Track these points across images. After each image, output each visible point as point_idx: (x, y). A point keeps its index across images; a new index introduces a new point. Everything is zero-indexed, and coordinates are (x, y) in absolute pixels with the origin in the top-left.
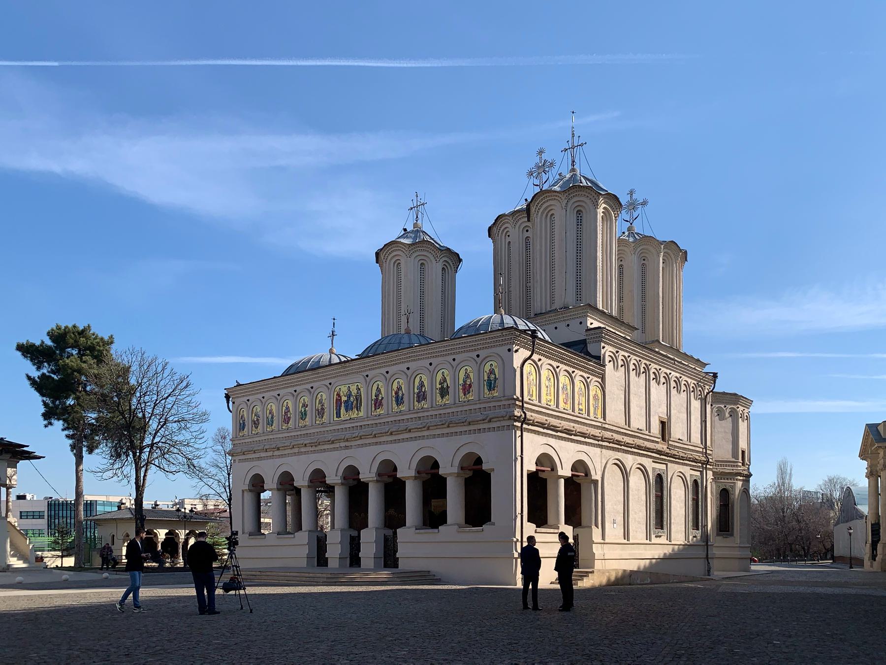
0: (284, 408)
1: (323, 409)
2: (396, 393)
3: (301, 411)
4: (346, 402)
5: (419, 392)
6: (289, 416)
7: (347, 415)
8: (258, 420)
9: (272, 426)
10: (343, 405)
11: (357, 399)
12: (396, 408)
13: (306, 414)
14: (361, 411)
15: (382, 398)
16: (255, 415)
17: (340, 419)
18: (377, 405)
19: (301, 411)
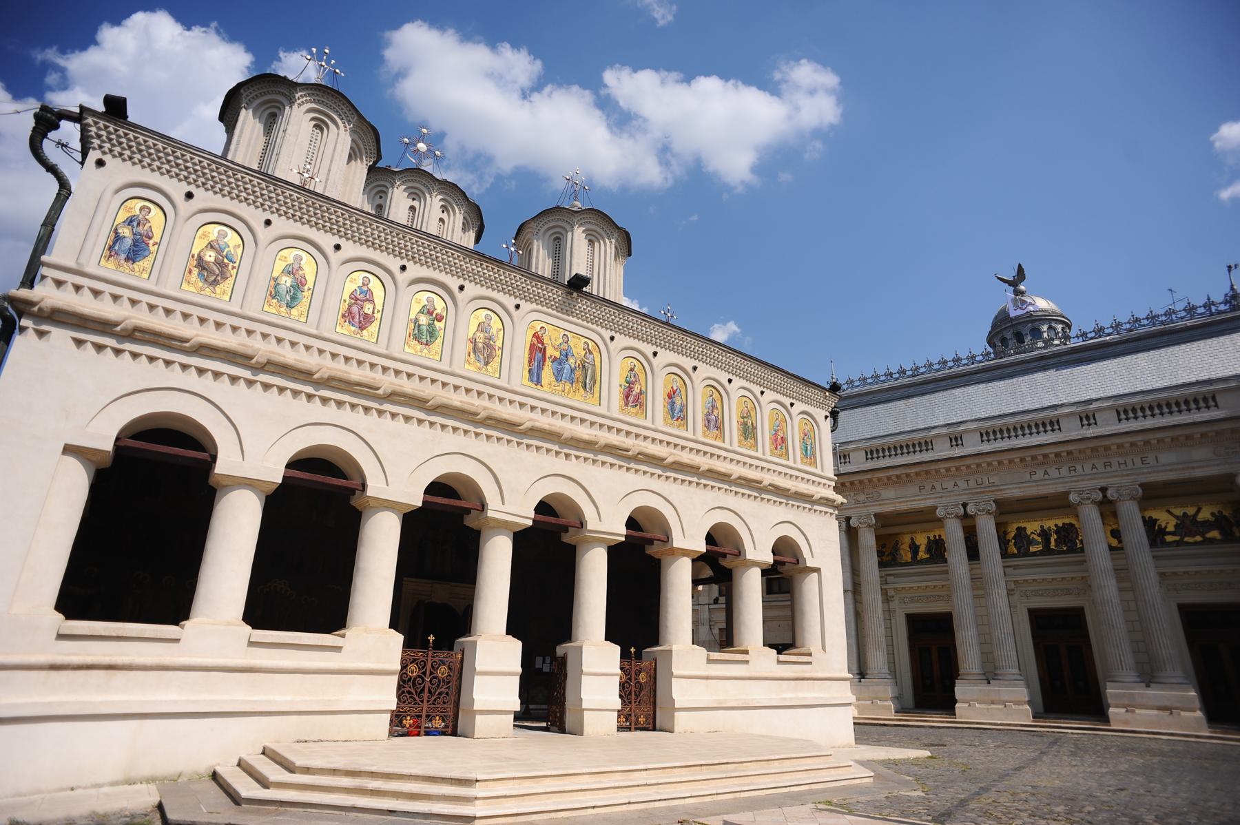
0: (350, 287)
1: (489, 345)
2: (670, 396)
3: (416, 320)
4: (555, 360)
5: (709, 414)
6: (370, 312)
7: (560, 388)
8: (221, 264)
9: (289, 306)
10: (548, 362)
11: (584, 367)
12: (670, 421)
13: (432, 333)
14: (593, 394)
15: (641, 393)
16: (211, 246)
17: (539, 387)
18: (631, 398)
19: (416, 320)
